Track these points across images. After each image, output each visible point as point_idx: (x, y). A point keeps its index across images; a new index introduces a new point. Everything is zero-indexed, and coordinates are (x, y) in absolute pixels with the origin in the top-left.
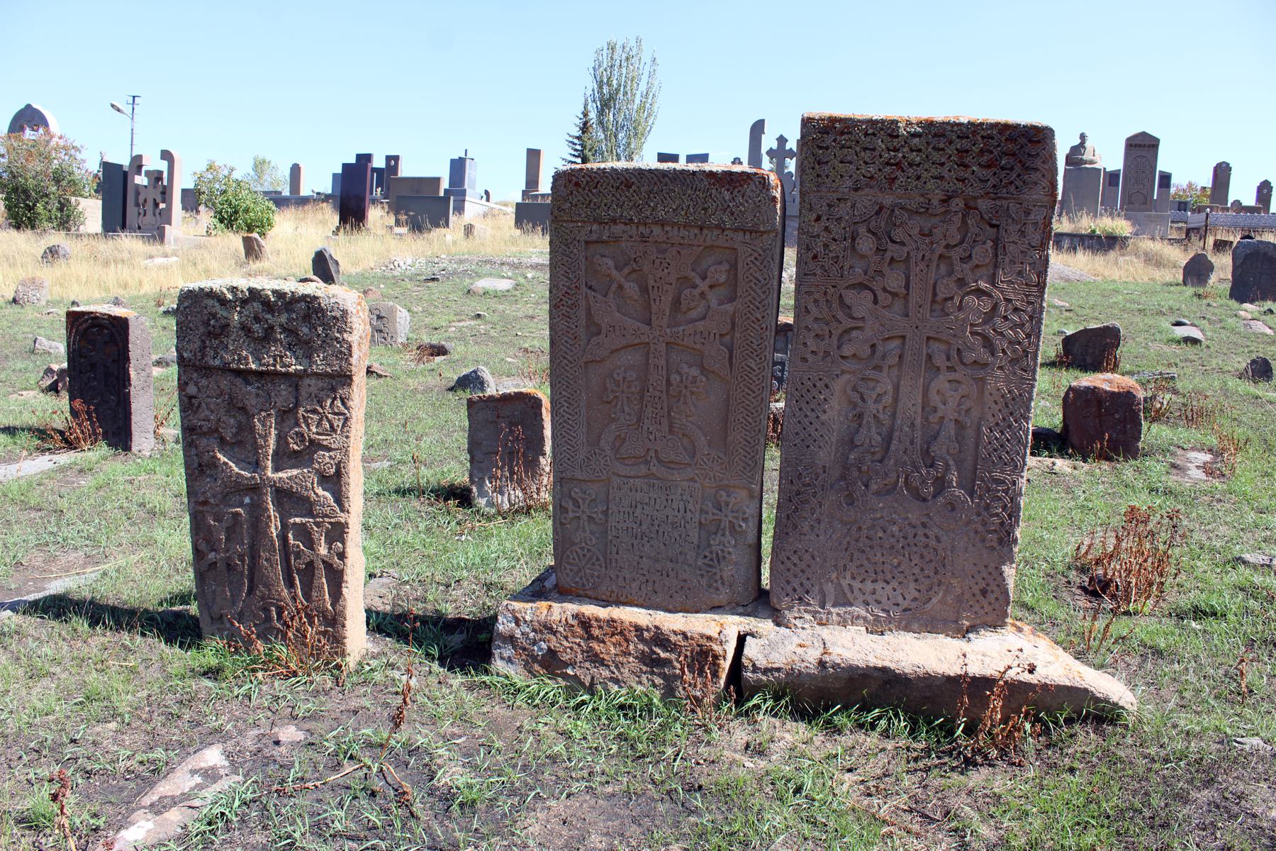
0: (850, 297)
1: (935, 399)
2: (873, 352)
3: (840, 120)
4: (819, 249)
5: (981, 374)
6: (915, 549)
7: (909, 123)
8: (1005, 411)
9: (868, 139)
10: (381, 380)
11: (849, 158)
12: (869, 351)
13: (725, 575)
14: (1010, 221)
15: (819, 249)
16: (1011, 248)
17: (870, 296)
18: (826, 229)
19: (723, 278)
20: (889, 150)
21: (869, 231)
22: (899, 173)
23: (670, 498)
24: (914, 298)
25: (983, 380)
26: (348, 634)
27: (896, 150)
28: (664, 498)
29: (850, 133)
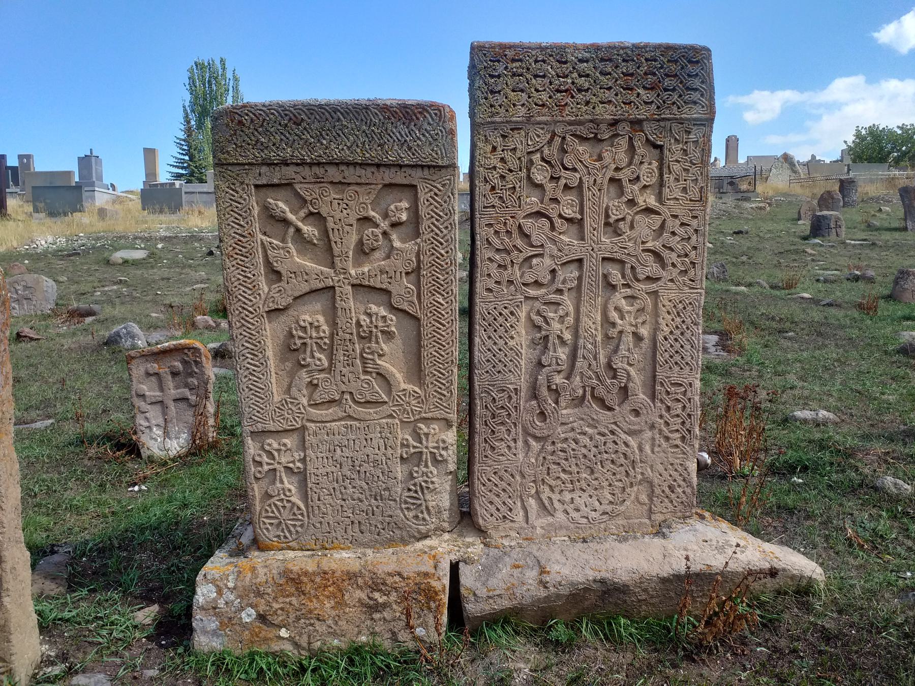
0: (528, 224)
1: (614, 315)
2: (554, 278)
3: (511, 47)
4: (497, 181)
5: (654, 286)
6: (605, 456)
7: (576, 47)
8: (678, 320)
9: (539, 65)
10: (33, 343)
11: (521, 86)
12: (549, 277)
13: (431, 504)
14: (673, 141)
15: (497, 181)
16: (676, 167)
17: (548, 224)
18: (503, 160)
19: (404, 217)
20: (559, 76)
21: (543, 159)
22: (569, 100)
23: (368, 437)
24: (588, 222)
25: (656, 293)
26: (14, 650)
27: (566, 76)
28: (362, 437)
29: (521, 60)
